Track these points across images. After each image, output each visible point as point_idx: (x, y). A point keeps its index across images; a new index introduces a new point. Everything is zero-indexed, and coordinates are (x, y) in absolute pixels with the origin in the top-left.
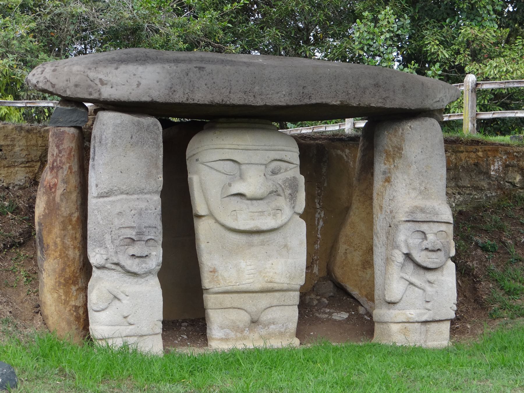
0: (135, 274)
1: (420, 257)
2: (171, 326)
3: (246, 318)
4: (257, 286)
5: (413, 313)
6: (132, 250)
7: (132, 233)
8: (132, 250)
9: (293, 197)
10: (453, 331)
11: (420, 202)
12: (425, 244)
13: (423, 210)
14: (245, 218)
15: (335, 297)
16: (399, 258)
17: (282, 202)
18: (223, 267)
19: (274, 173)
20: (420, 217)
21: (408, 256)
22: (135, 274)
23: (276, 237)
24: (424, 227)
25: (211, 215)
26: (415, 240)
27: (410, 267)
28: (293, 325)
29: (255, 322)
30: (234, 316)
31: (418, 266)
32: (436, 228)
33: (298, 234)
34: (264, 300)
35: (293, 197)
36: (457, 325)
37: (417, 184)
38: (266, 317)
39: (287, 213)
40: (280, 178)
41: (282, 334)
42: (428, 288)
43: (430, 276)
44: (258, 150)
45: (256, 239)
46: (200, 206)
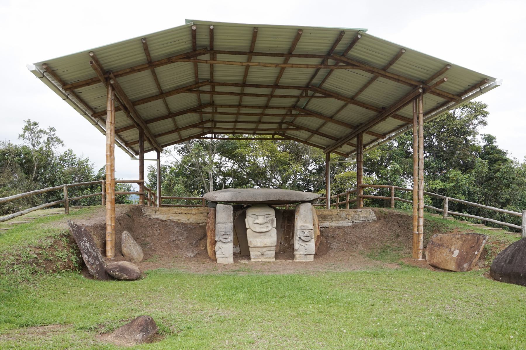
0: (224, 243)
1: (303, 238)
2: (236, 256)
3: (260, 253)
4: (262, 246)
5: (301, 253)
6: (224, 237)
7: (223, 233)
8: (224, 237)
9: (272, 224)
10: (315, 258)
11: (303, 224)
12: (305, 235)
13: (304, 226)
14: (258, 229)
15: (285, 249)
16: (298, 238)
17: (269, 225)
18: (253, 240)
19: (267, 217)
20: (303, 228)
21: (300, 238)
22: (224, 243)
23: (268, 234)
24: (304, 231)
25: (250, 228)
26: (302, 234)
27: (301, 241)
28: (273, 255)
29: (262, 255)
30: (257, 253)
31: (303, 240)
32: (308, 231)
33: (274, 233)
34: (265, 249)
35: (272, 224)
36: (316, 255)
37: (303, 219)
38: (265, 253)
39: (270, 227)
40: (269, 219)
41: (270, 258)
42: (306, 246)
43: (307, 243)
44: (37, 210)
45: (262, 234)
46: (247, 227)
